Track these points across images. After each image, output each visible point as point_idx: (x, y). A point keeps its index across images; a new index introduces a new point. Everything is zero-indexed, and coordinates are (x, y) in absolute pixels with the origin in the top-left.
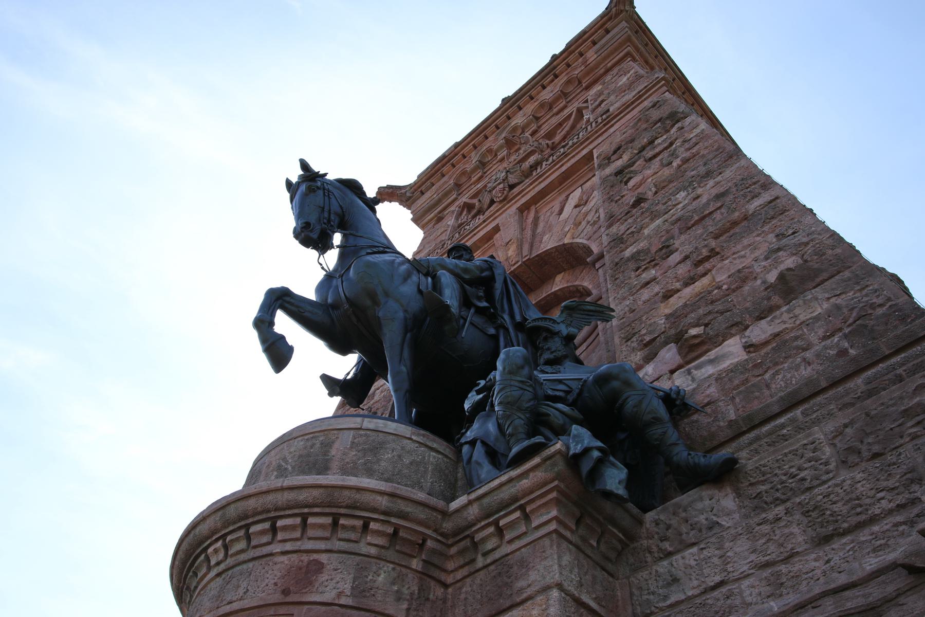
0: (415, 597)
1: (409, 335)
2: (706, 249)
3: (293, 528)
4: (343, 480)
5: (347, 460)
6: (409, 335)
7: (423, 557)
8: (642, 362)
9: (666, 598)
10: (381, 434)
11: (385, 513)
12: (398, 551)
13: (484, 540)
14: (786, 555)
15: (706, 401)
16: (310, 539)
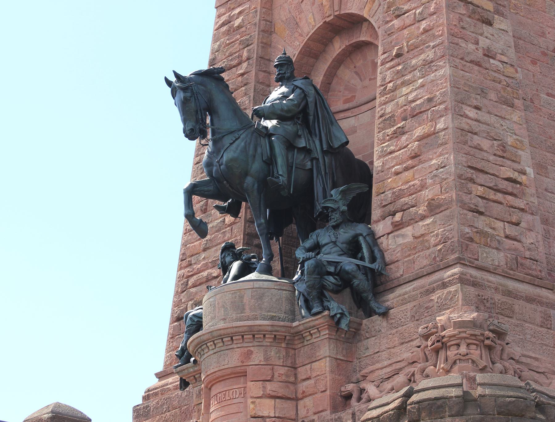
0: (285, 357)
1: (262, 195)
2: (414, 151)
3: (239, 339)
4: (254, 323)
6: (262, 195)
7: (286, 342)
8: (380, 218)
9: (365, 354)
10: (262, 289)
13: (306, 336)
14: (393, 346)
15: (396, 260)
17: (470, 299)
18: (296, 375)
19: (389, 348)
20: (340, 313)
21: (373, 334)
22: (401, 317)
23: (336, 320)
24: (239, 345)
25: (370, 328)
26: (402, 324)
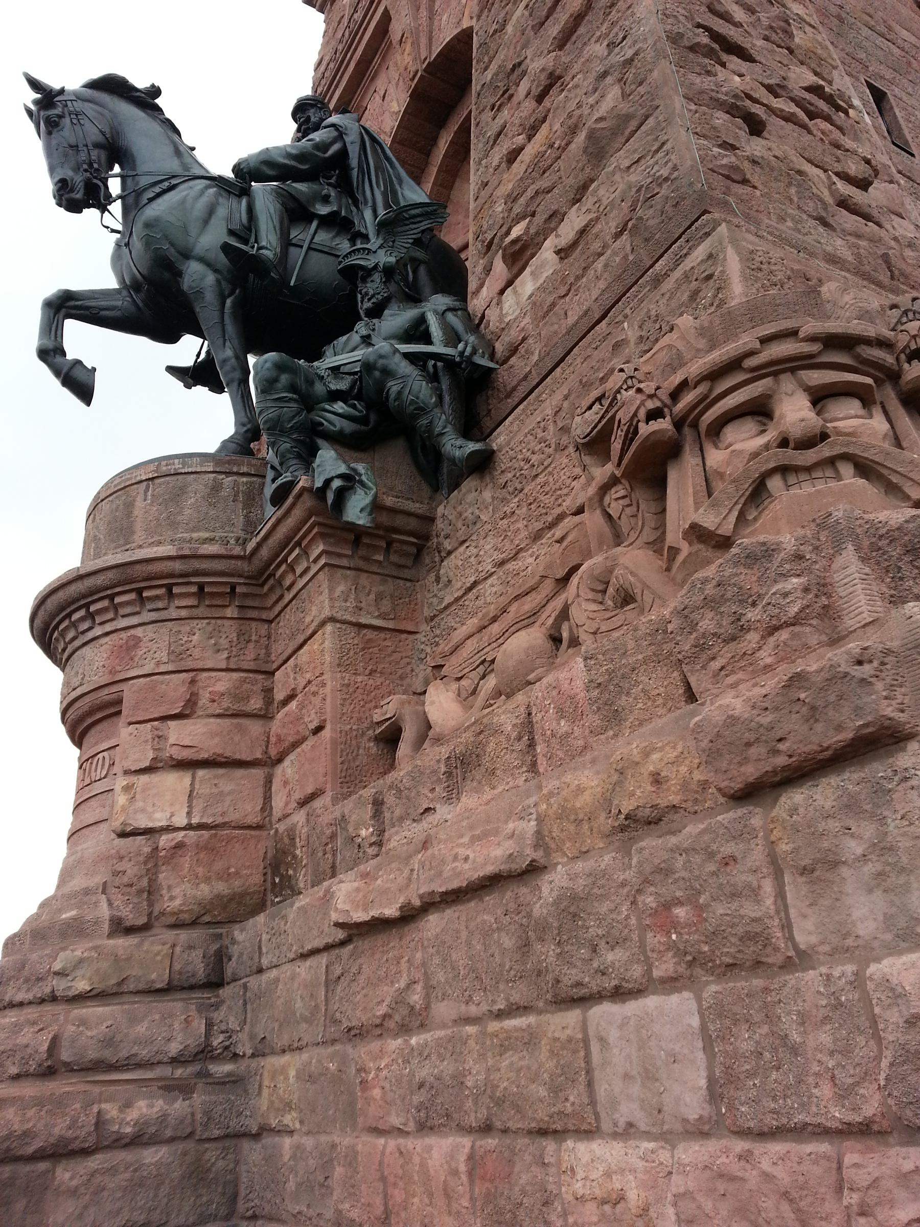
0: (234, 644)
1: (229, 302)
4: (131, 556)
5: (150, 518)
6: (229, 302)
11: (182, 576)
12: (208, 606)
14: (514, 552)
15: (520, 338)
16: (123, 616)
17: (775, 279)
18: (268, 692)
19: (502, 563)
20: (341, 476)
21: (461, 535)
22: (529, 454)
23: (330, 497)
24: (108, 627)
25: (454, 521)
26: (534, 473)
